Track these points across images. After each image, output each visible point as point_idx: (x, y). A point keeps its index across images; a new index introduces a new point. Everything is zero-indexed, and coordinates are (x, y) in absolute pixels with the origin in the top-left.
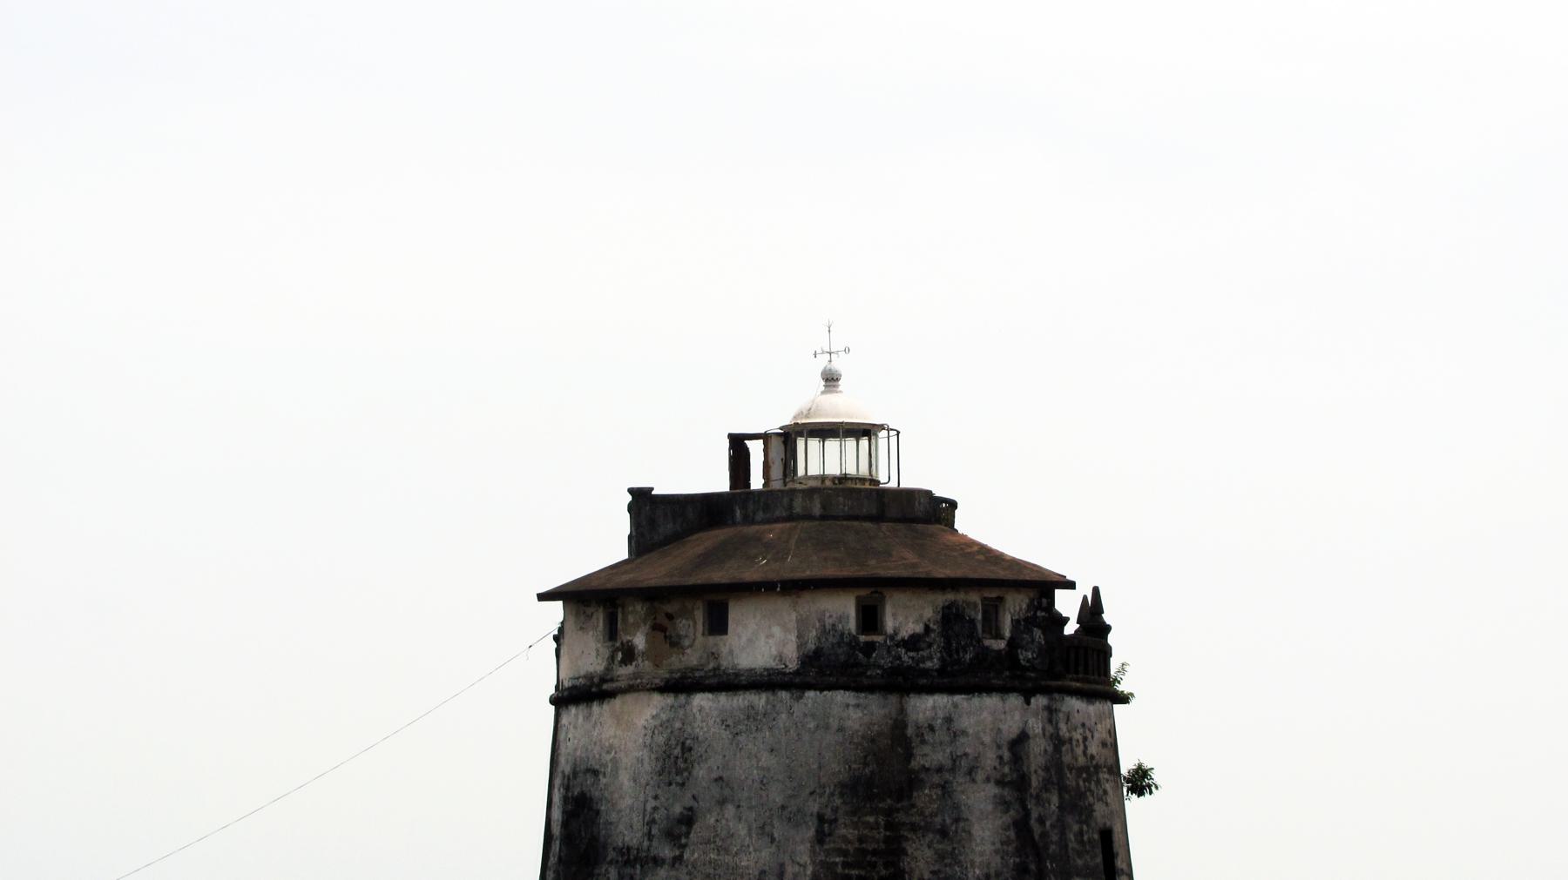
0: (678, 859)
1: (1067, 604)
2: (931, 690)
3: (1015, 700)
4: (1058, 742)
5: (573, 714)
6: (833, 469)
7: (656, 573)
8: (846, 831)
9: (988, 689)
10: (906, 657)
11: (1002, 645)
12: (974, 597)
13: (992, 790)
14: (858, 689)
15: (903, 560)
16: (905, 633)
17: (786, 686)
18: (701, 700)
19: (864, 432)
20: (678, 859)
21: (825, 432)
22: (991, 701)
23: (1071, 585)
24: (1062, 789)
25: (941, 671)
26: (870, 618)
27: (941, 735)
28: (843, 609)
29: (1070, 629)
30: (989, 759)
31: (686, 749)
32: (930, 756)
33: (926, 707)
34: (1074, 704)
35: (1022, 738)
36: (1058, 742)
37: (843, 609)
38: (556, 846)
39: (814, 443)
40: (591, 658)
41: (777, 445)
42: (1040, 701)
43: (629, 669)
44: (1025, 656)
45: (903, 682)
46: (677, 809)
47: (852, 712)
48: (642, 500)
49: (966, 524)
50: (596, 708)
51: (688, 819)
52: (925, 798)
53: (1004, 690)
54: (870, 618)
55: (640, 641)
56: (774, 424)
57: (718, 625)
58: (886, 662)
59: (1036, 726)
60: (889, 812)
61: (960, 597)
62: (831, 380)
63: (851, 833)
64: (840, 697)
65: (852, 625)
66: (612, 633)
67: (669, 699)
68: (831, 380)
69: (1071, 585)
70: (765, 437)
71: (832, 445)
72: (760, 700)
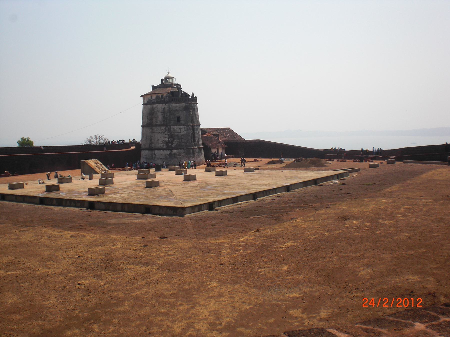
3: (164, 104)
4: (170, 108)
12: (160, 95)
22: (161, 105)
28: (150, 96)
30: (161, 110)
32: (155, 110)
33: (155, 106)
35: (165, 108)
36: (170, 108)
37: (150, 96)
45: (153, 103)
47: (149, 106)
48: (153, 87)
59: (166, 107)
61: (158, 95)
62: (169, 73)
68: (169, 73)
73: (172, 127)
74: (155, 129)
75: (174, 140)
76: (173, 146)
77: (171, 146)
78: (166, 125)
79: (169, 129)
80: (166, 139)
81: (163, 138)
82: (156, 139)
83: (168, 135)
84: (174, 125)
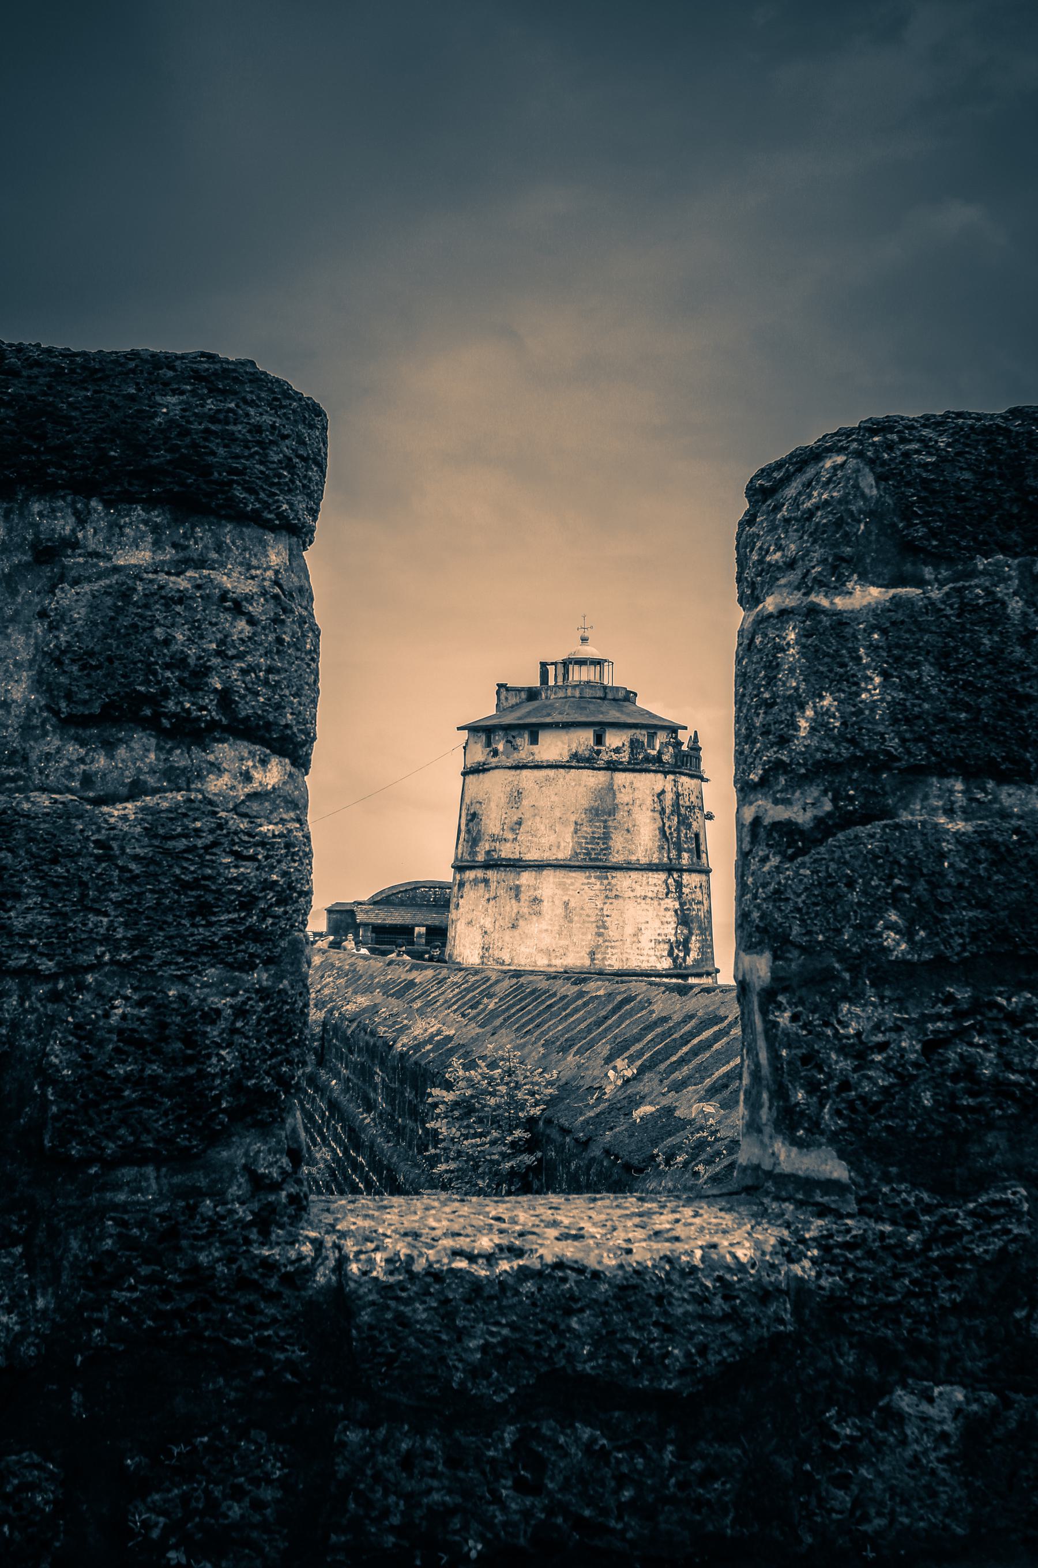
0: (515, 839)
1: (684, 736)
2: (624, 770)
3: (660, 776)
4: (678, 795)
5: (470, 778)
6: (584, 678)
7: (509, 719)
8: (586, 829)
9: (647, 771)
10: (615, 757)
11: (654, 753)
12: (644, 732)
13: (650, 814)
14: (594, 769)
15: (613, 715)
16: (614, 746)
17: (563, 767)
18: (525, 773)
19: (598, 663)
20: (515, 839)
21: (581, 662)
23: (685, 728)
24: (679, 815)
25: (629, 763)
26: (599, 740)
27: (628, 790)
29: (685, 748)
30: (649, 801)
31: (519, 793)
32: (623, 798)
33: (621, 778)
34: (684, 779)
35: (663, 792)
38: (463, 835)
39: (576, 667)
40: (479, 754)
41: (560, 667)
42: (671, 777)
43: (496, 759)
44: (665, 758)
45: (612, 767)
46: (515, 819)
47: (593, 779)
49: (640, 703)
50: (481, 775)
51: (519, 823)
52: (621, 814)
53: (656, 772)
54: (599, 740)
55: (501, 747)
56: (560, 657)
57: (534, 741)
58: (606, 758)
59: (669, 787)
60: (605, 821)
63: (589, 830)
64: (586, 772)
65: (592, 743)
66: (488, 744)
67: (513, 772)
69: (685, 728)
70: (555, 664)
71: (584, 668)
72: (551, 773)
73: (686, 877)
74: (623, 881)
75: (691, 934)
76: (689, 961)
77: (685, 960)
78: (669, 869)
79: (679, 885)
80: (670, 930)
81: (657, 924)
82: (629, 930)
83: (676, 911)
84: (690, 871)
